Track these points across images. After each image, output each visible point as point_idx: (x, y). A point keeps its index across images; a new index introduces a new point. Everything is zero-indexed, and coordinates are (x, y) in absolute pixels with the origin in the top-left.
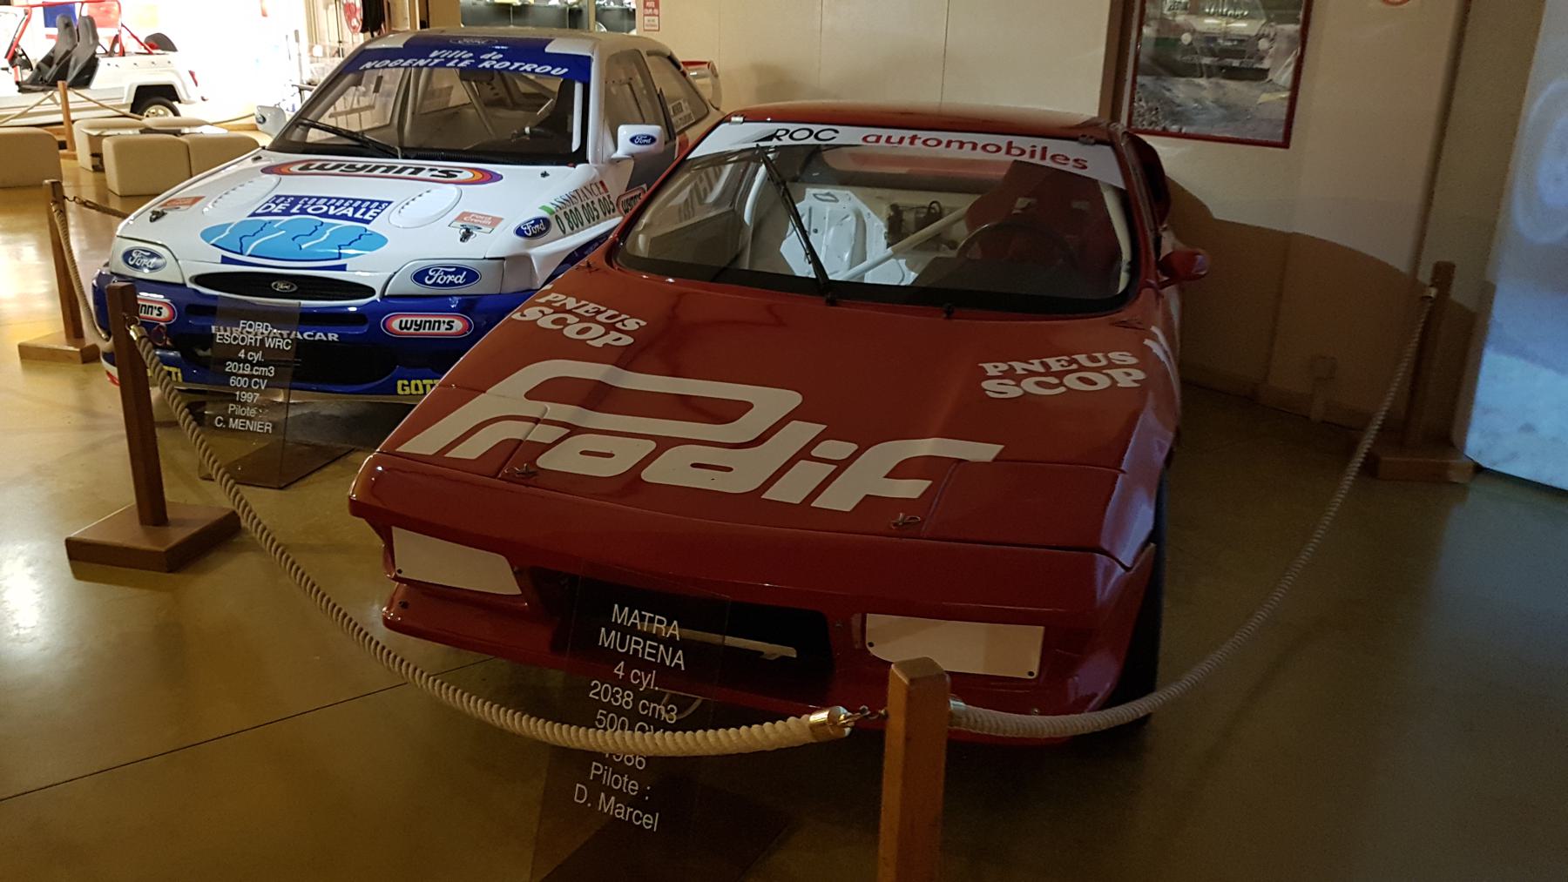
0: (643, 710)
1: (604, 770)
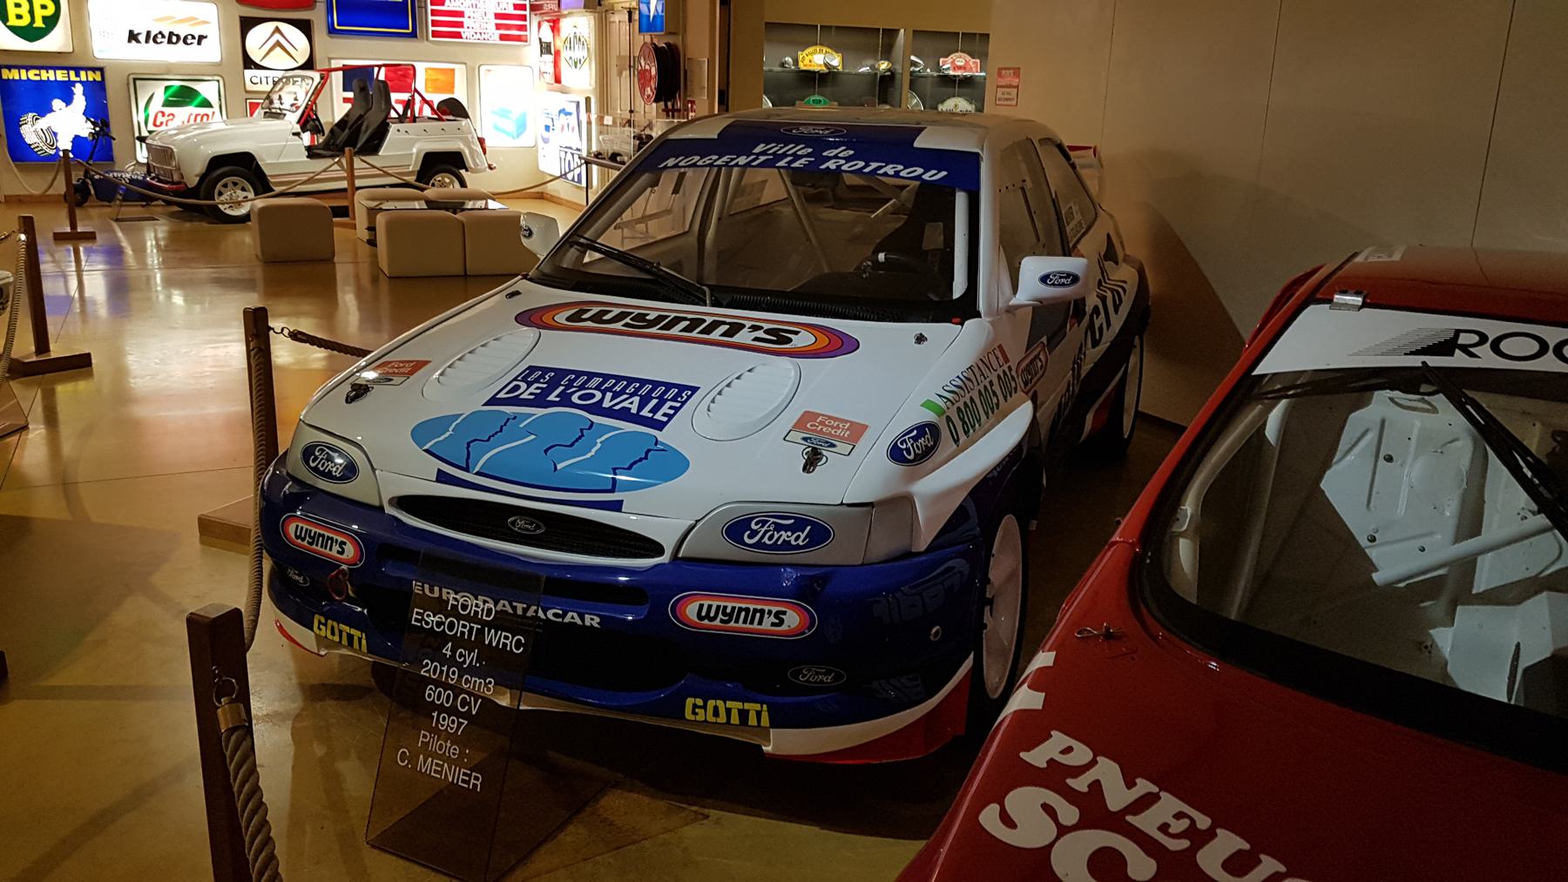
1: (431, 737)
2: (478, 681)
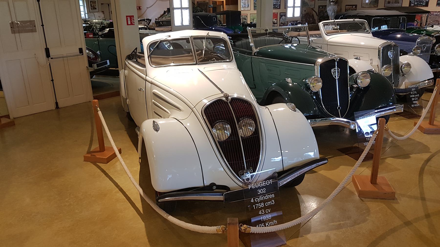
0: (267, 205)
2: (270, 202)
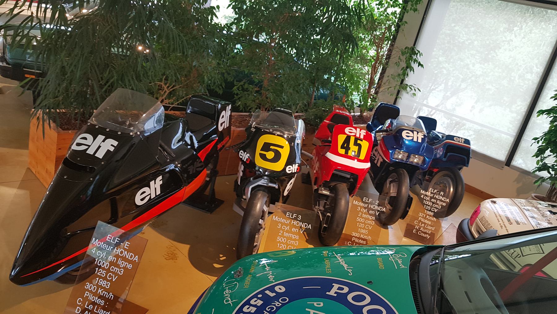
0: (112, 269)
2: (117, 269)
